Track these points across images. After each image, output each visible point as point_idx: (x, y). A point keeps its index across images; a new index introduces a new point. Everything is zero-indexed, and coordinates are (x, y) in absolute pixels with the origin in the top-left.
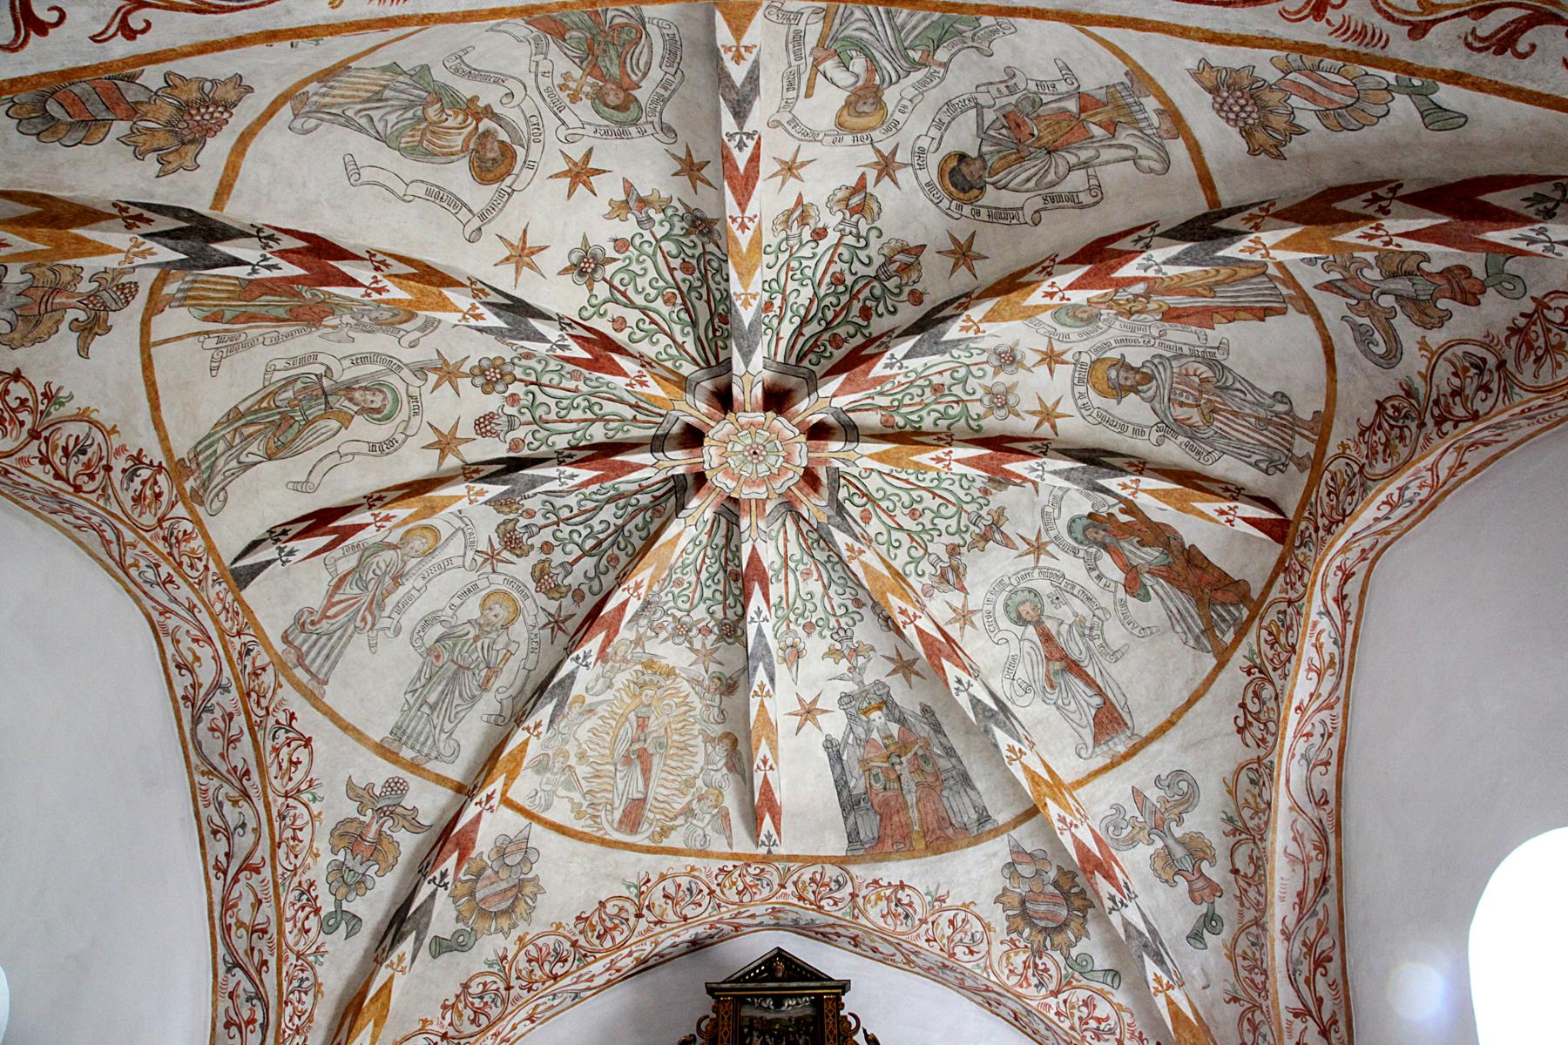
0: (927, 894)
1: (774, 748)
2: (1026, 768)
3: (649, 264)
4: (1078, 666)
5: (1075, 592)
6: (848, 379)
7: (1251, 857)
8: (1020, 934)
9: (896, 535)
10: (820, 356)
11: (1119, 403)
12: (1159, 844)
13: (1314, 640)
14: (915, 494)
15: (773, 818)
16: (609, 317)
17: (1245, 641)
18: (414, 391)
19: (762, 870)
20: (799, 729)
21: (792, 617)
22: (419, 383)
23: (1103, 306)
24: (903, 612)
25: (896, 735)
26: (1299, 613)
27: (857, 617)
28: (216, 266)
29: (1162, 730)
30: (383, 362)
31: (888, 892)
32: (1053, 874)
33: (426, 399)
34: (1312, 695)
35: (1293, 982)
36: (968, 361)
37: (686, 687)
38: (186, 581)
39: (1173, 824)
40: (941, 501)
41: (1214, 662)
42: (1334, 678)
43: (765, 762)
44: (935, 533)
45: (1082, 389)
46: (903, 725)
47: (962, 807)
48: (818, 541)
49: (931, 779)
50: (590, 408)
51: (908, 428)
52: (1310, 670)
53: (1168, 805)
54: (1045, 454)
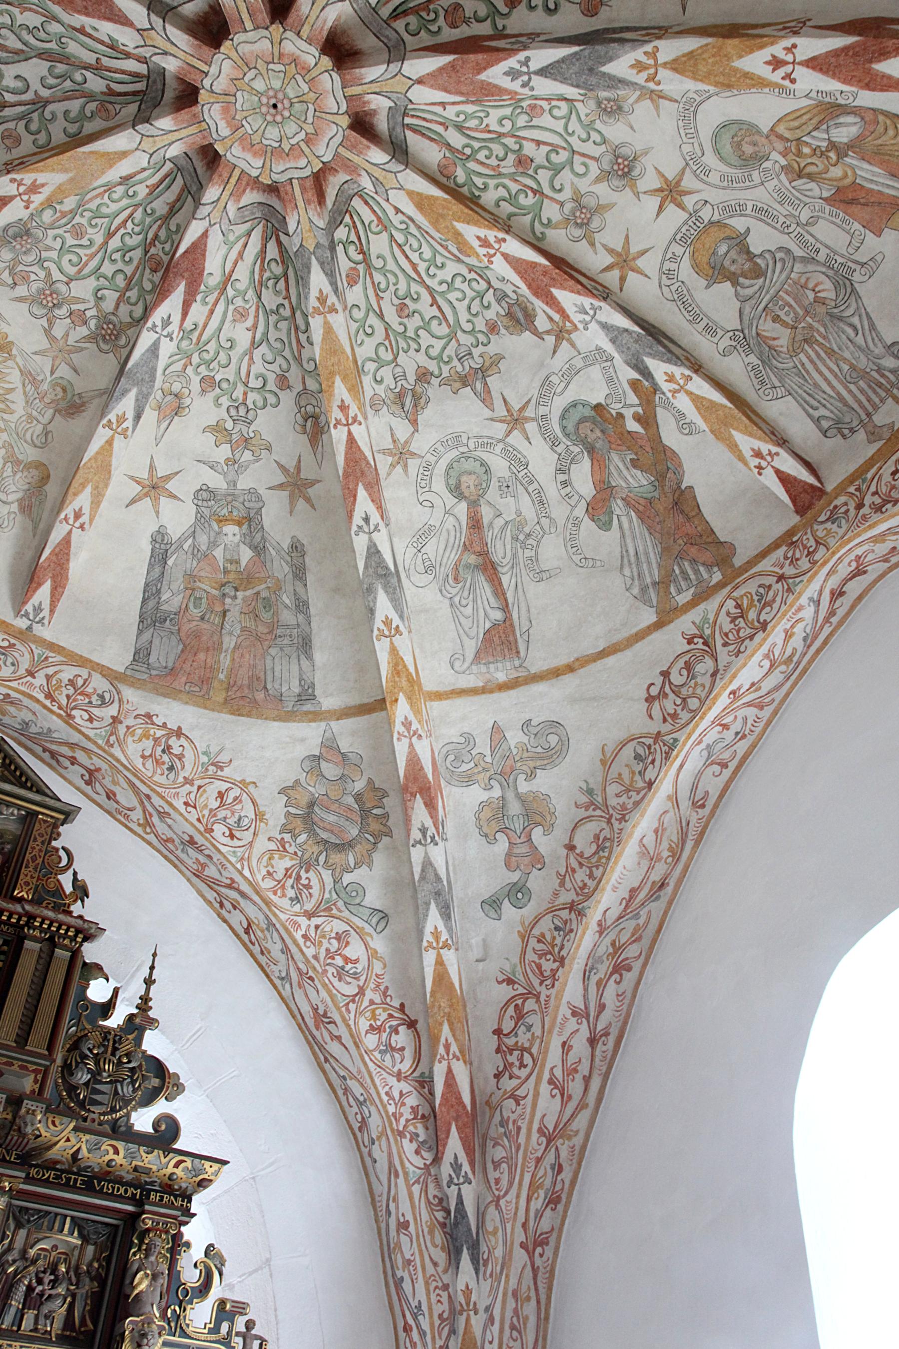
0: (204, 753)
1: (96, 503)
2: (394, 651)
4: (495, 569)
5: (530, 489)
6: (452, 65)
7: (597, 837)
8: (295, 837)
9: (373, 320)
10: (424, 25)
11: (707, 287)
12: (497, 792)
13: (788, 627)
14: (415, 288)
15: (54, 589)
17: (702, 606)
19: (12, 646)
20: (133, 501)
21: (195, 359)
23: (780, 146)
24: (343, 408)
25: (243, 564)
26: (789, 590)
27: (272, 399)
29: (556, 673)
31: (159, 733)
32: (359, 785)
34: (753, 684)
35: (585, 978)
36: (577, 145)
37: (15, 378)
39: (522, 777)
40: (438, 314)
41: (653, 618)
42: (783, 676)
43: (78, 515)
44: (414, 346)
45: (678, 250)
46: (259, 555)
47: (286, 674)
48: (277, 279)
49: (262, 629)
51: (465, 190)
52: (767, 656)
53: (525, 755)
54: (605, 299)
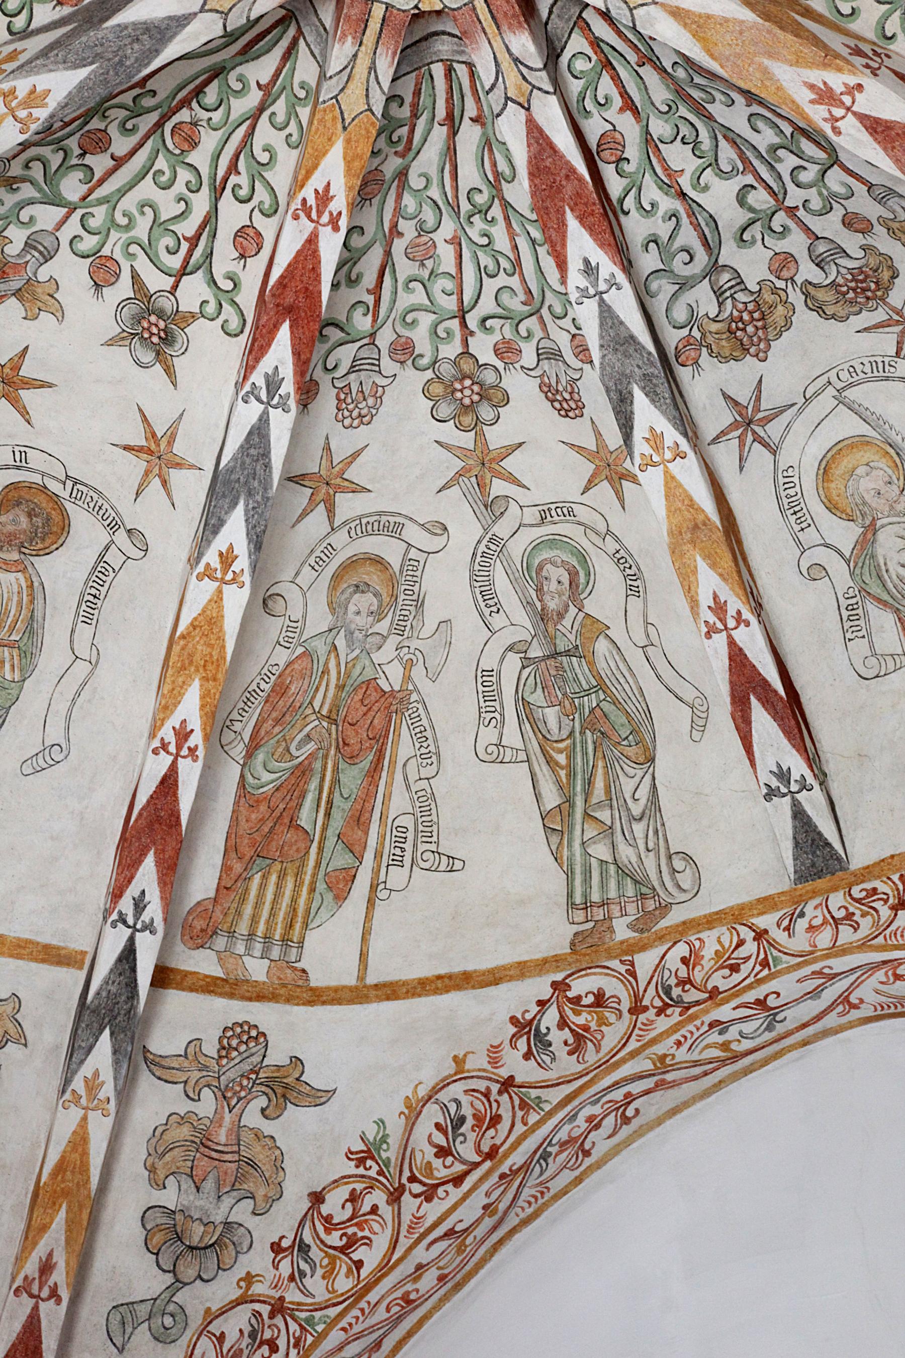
3: (129, 202)
16: (235, 267)
18: (531, 516)
22: (513, 508)
28: (132, 984)
30: (486, 567)
33: (540, 495)
38: (750, 987)
50: (484, 211)
